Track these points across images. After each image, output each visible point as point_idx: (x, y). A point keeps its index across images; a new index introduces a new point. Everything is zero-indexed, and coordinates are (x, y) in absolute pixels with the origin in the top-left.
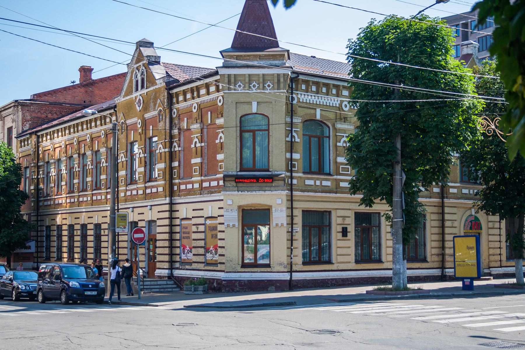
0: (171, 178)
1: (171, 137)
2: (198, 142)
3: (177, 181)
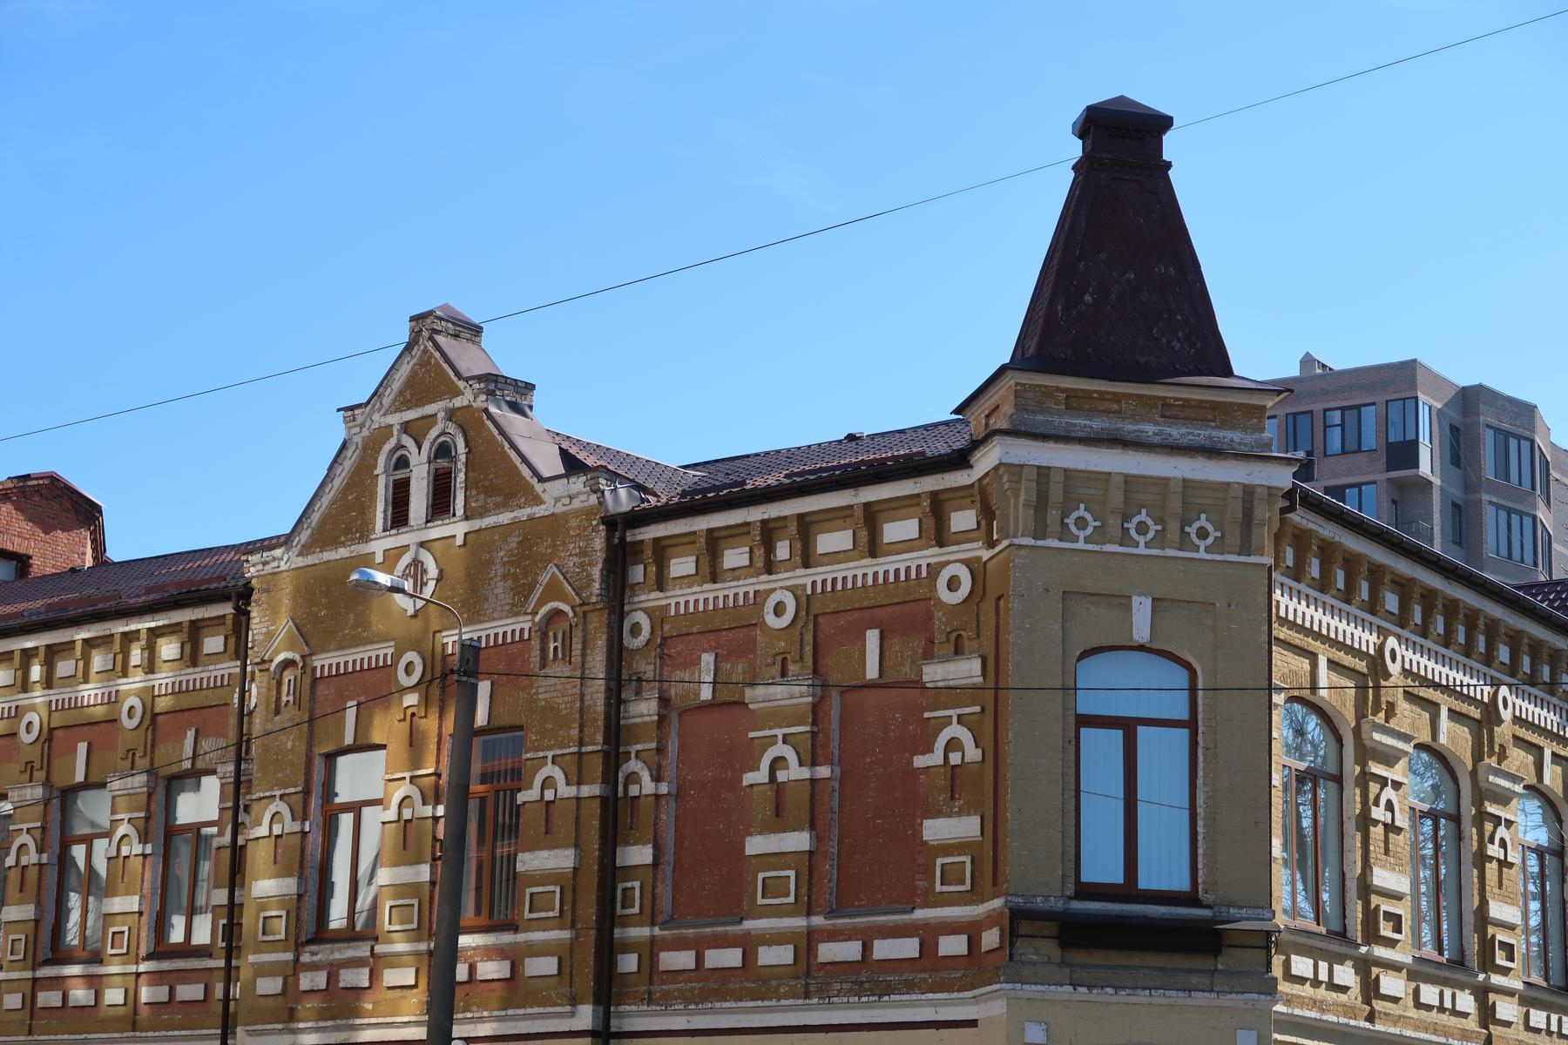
0: (608, 919)
1: (616, 734)
2: (792, 758)
3: (640, 932)
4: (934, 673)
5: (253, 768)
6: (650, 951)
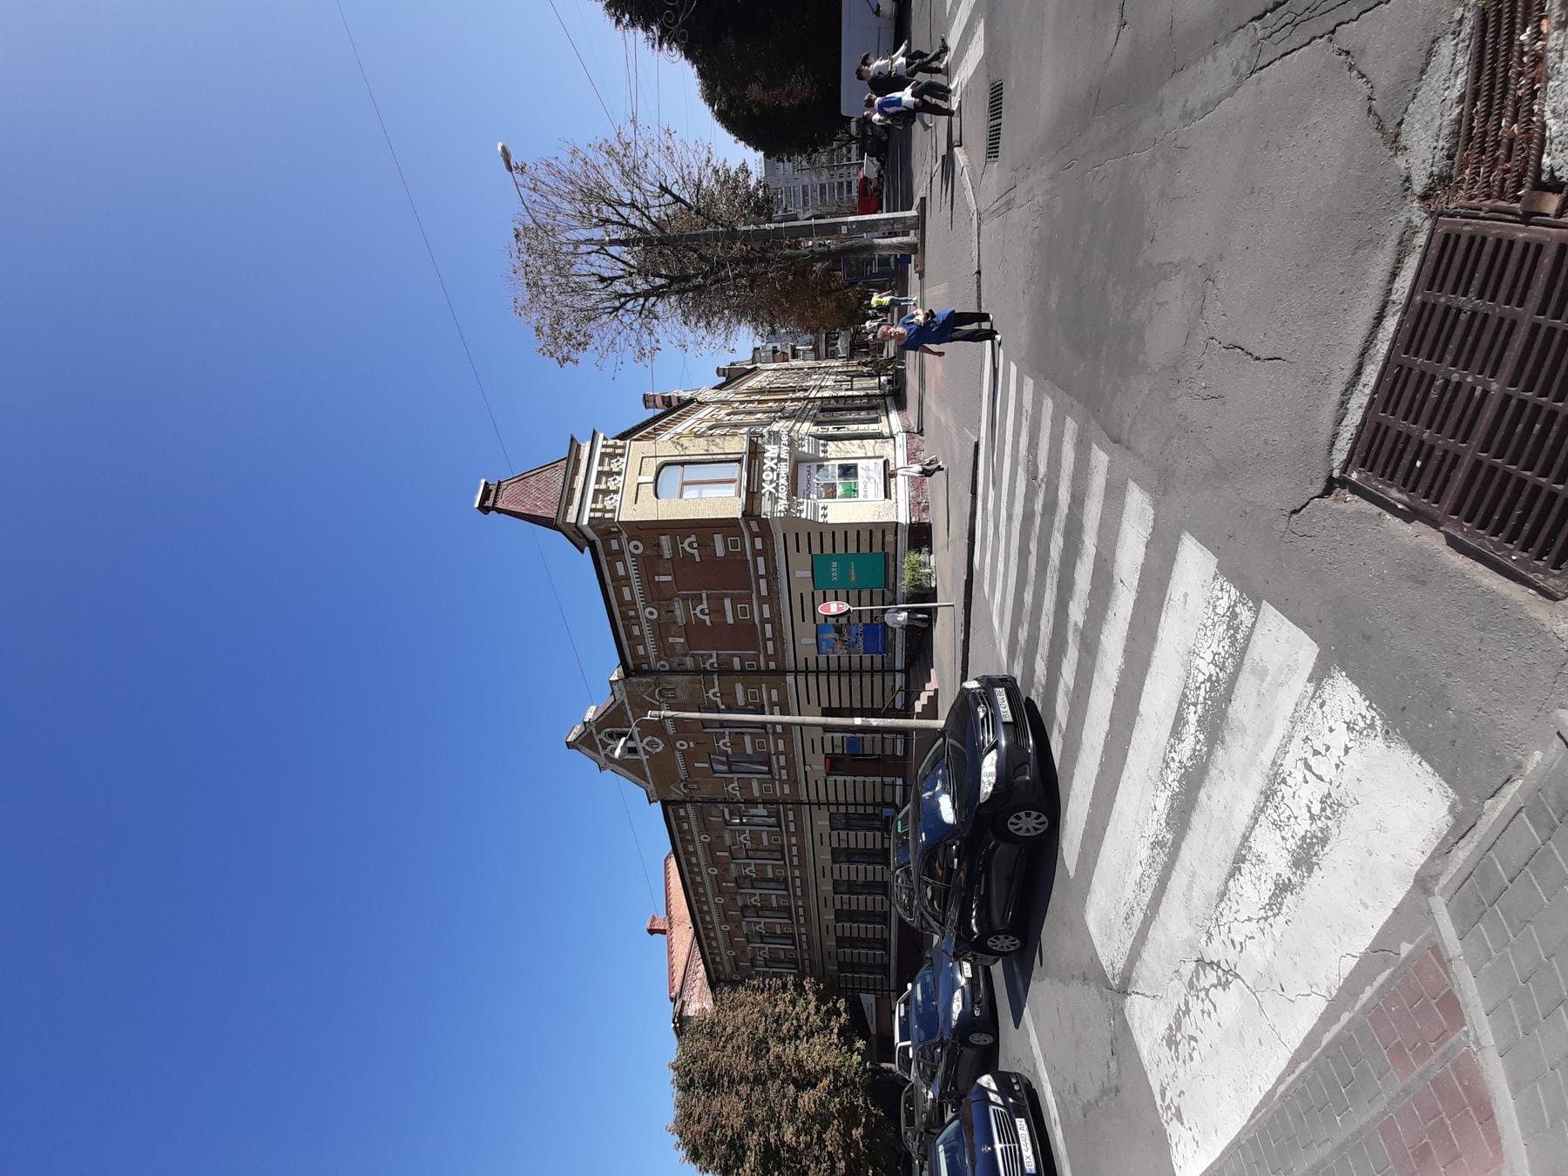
0: (759, 672)
1: (697, 672)
4: (667, 554)
5: (720, 797)
6: (768, 658)
